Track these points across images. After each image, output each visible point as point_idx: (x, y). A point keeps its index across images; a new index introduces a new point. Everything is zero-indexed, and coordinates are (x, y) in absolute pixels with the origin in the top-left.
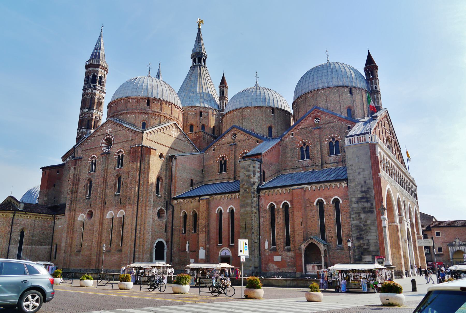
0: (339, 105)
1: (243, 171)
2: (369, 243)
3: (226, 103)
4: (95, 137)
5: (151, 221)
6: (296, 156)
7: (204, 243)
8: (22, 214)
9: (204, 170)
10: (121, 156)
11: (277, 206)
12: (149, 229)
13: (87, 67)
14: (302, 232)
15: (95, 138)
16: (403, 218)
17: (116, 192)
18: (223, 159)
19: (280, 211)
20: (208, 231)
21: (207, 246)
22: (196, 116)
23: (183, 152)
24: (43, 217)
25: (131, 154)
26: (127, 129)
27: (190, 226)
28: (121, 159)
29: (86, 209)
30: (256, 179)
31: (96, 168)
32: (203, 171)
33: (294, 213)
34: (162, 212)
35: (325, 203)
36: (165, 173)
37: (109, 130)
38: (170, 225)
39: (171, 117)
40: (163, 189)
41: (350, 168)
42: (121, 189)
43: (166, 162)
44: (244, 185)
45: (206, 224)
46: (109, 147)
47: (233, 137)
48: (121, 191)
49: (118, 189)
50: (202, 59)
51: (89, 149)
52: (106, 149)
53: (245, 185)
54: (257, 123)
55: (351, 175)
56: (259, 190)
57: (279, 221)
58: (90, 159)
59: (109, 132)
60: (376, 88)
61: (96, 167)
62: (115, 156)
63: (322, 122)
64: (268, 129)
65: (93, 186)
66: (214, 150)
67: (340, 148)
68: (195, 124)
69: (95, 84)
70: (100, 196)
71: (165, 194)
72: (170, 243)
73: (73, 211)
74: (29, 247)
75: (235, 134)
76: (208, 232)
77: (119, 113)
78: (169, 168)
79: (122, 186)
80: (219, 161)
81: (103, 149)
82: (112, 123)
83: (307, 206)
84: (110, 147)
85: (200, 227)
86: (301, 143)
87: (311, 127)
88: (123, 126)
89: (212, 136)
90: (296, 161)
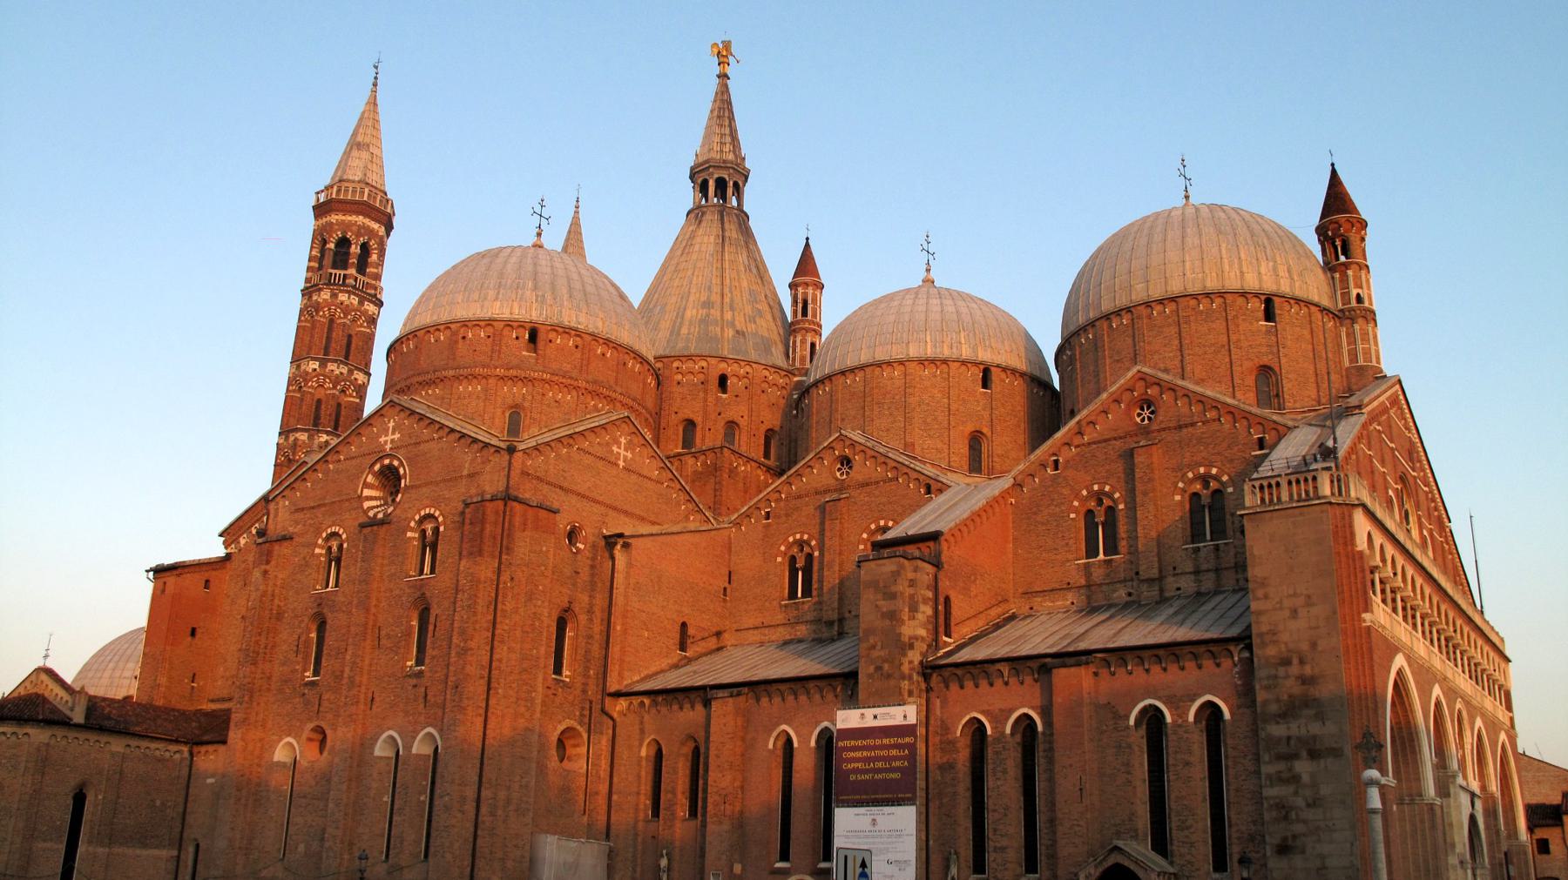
0: (1227, 360)
2: (1324, 867)
3: (813, 345)
4: (340, 461)
6: (1067, 544)
7: (724, 857)
9: (728, 591)
10: (429, 532)
11: (992, 728)
13: (320, 210)
14: (1081, 823)
15: (340, 466)
16: (1454, 777)
17: (409, 663)
19: (1003, 747)
21: (738, 868)
22: (706, 392)
23: (654, 523)
25: (467, 527)
26: (458, 435)
28: (430, 544)
30: (916, 627)
31: (341, 575)
32: (725, 594)
33: (1056, 754)
34: (572, 742)
35: (1169, 719)
36: (586, 599)
39: (614, 395)
40: (578, 658)
41: (1260, 593)
42: (429, 652)
43: (594, 559)
44: (873, 647)
46: (390, 500)
47: (839, 470)
48: (427, 661)
49: (418, 651)
51: (319, 506)
52: (377, 507)
53: (879, 647)
54: (925, 422)
55: (1263, 619)
56: (928, 670)
57: (999, 783)
58: (320, 541)
59: (388, 447)
60: (1359, 299)
61: (342, 570)
62: (409, 534)
63: (1162, 422)
64: (967, 442)
65: (330, 641)
66: (768, 516)
67: (1228, 517)
68: (698, 420)
69: (346, 272)
70: (352, 674)
71: (586, 676)
74: (100, 850)
75: (846, 461)
79: (433, 643)
80: (783, 559)
81: (367, 504)
82: (402, 415)
83: (1105, 728)
84: (394, 500)
85: (710, 800)
86: (1087, 498)
87: (1121, 438)
88: (442, 426)
89: (760, 464)
90: (1068, 561)
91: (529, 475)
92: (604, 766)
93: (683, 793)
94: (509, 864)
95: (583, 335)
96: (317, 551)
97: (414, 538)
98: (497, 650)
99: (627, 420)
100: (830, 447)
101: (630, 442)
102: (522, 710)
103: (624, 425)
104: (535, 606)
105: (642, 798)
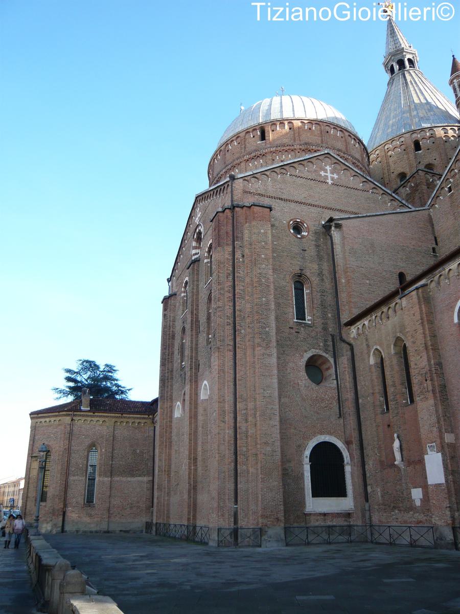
5: (276, 385)
7: (435, 429)
8: (88, 416)
12: (270, 407)
20: (444, 387)
22: (407, 154)
24: (131, 421)
27: (394, 385)
29: (181, 391)
36: (316, 267)
38: (349, 396)
45: (430, 365)
66: (450, 189)
71: (324, 316)
72: (355, 446)
73: (167, 400)
76: (441, 392)
78: (328, 254)
91: (250, 193)
92: (348, 379)
93: (402, 384)
94: (260, 457)
95: (292, 121)
96: (183, 295)
98: (236, 305)
99: (328, 156)
102: (257, 340)
103: (327, 159)
104: (260, 268)
105: (378, 396)
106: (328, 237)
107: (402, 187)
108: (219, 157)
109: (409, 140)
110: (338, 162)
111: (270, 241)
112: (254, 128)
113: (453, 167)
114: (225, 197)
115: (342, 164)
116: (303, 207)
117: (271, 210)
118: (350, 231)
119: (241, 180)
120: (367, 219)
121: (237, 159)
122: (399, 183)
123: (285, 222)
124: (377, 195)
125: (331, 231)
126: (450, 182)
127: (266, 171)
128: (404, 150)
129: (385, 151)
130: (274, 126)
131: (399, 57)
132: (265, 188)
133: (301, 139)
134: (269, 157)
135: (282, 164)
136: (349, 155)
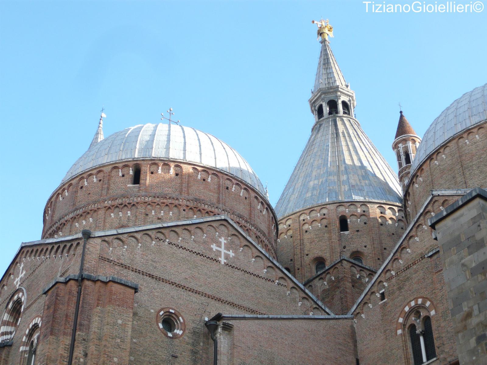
1: (455, 258)
18: (418, 314)
22: (329, 232)
37: (20, 276)
44: (469, 315)
50: (340, 102)
66: (383, 296)
68: (326, 255)
77: (54, 228)
80: (404, 330)
91: (109, 261)
95: (181, 165)
97: (25, 351)
100: (426, 213)
101: (232, 242)
103: (223, 228)
106: (211, 341)
107: (317, 279)
108: (67, 194)
109: (333, 213)
110: (237, 234)
111: (129, 337)
112: (126, 163)
113: (389, 267)
114: (70, 260)
115: (242, 238)
116: (181, 291)
117: (136, 292)
118: (243, 336)
119: (99, 240)
120: (267, 322)
121: (95, 203)
122: (314, 274)
123: (152, 311)
124: (285, 289)
125: (216, 334)
126: (384, 287)
127: (136, 232)
128: (326, 226)
129: (299, 222)
130: (153, 168)
131: (331, 97)
132: (132, 257)
133: (190, 192)
134: (141, 209)
135: (160, 226)
136: (253, 225)
